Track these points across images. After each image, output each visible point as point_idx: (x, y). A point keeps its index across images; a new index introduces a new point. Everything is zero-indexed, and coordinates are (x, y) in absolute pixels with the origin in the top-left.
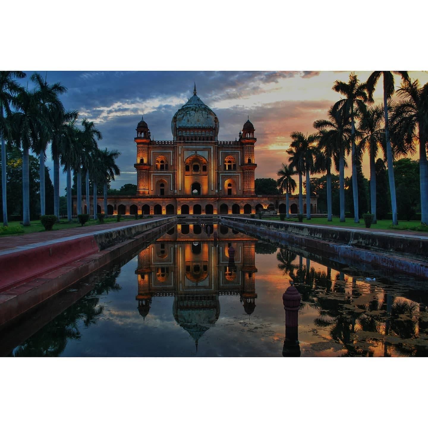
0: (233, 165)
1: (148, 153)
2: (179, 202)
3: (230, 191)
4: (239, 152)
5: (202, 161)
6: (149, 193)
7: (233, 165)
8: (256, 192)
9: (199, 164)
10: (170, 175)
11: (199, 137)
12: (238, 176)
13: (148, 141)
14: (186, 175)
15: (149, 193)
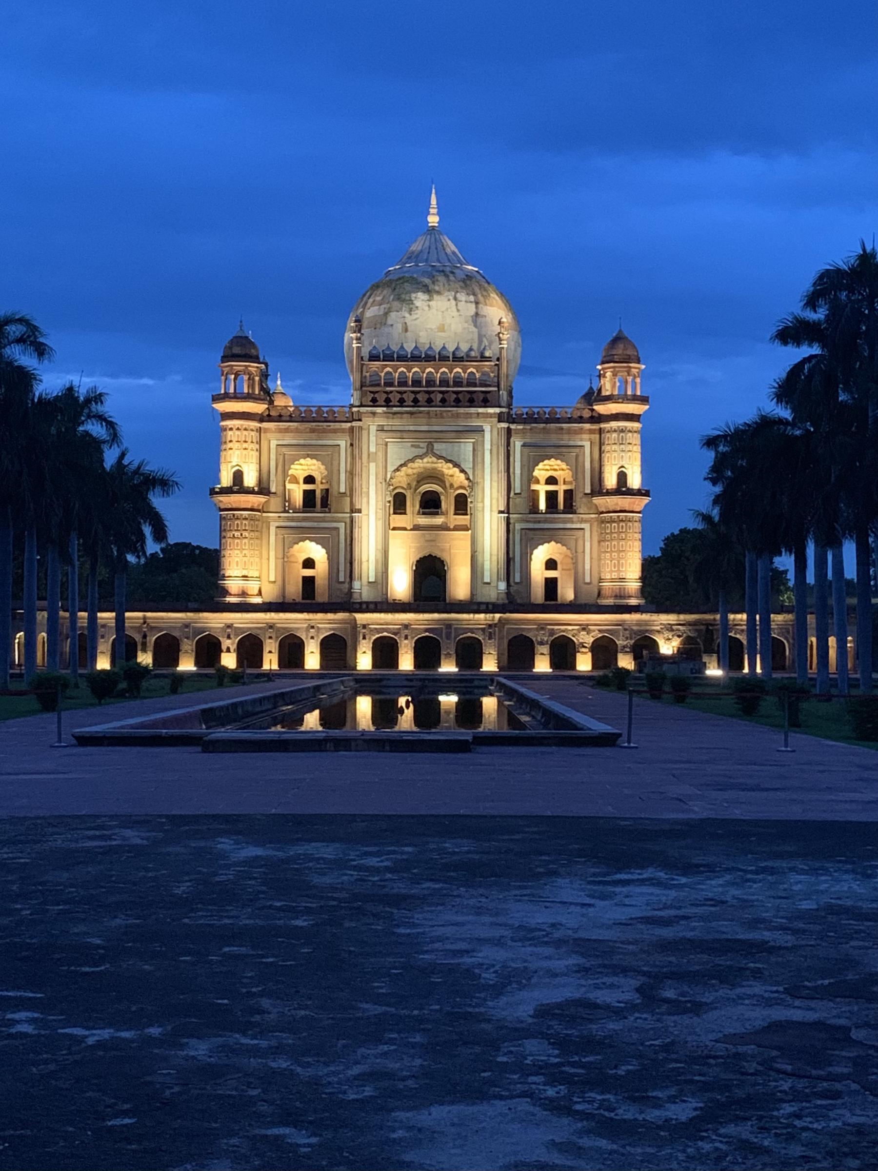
0: (566, 492)
1: (260, 451)
2: (364, 626)
3: (551, 585)
4: (587, 445)
5: (452, 476)
6: (260, 593)
7: (566, 492)
8: (643, 592)
9: (439, 489)
10: (337, 529)
11: (441, 392)
12: (580, 533)
13: (259, 408)
14: (394, 529)
15: (260, 593)
